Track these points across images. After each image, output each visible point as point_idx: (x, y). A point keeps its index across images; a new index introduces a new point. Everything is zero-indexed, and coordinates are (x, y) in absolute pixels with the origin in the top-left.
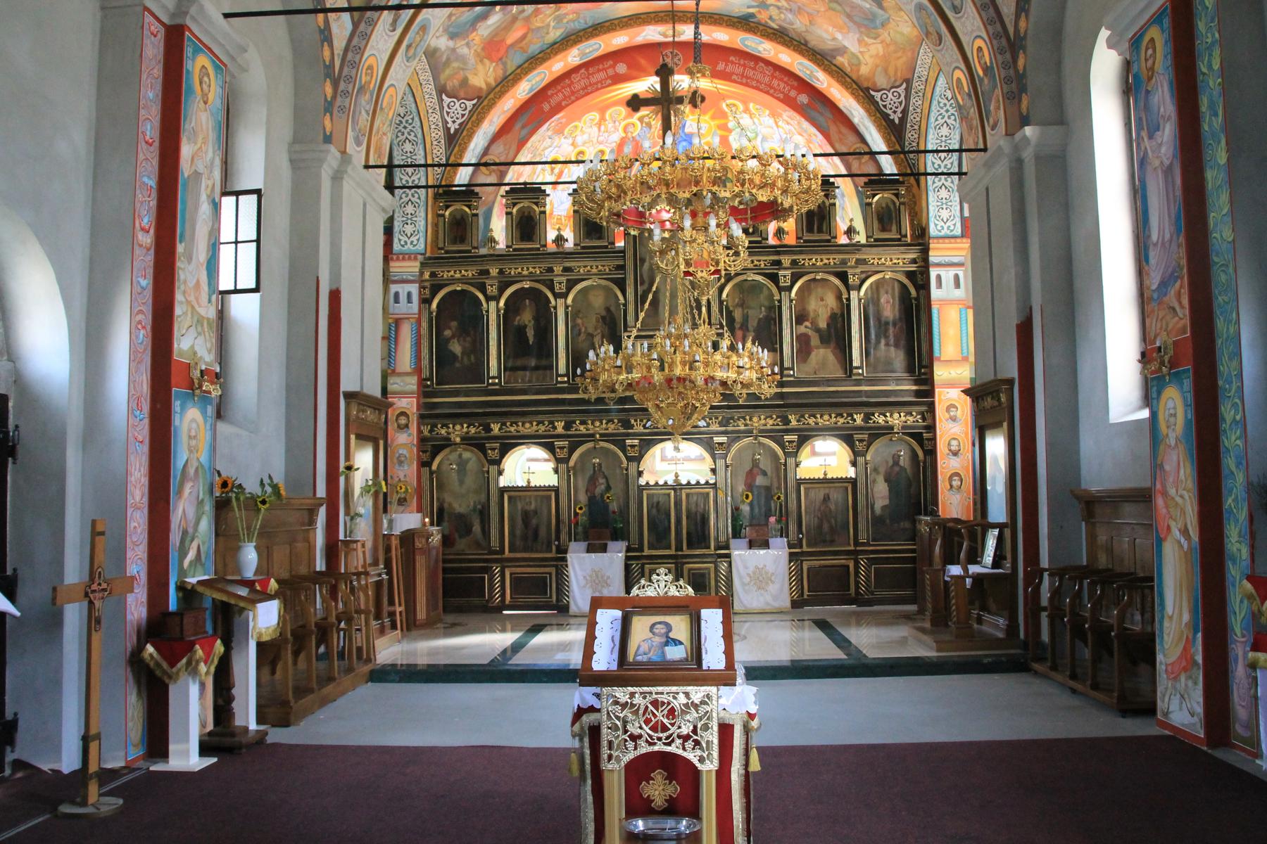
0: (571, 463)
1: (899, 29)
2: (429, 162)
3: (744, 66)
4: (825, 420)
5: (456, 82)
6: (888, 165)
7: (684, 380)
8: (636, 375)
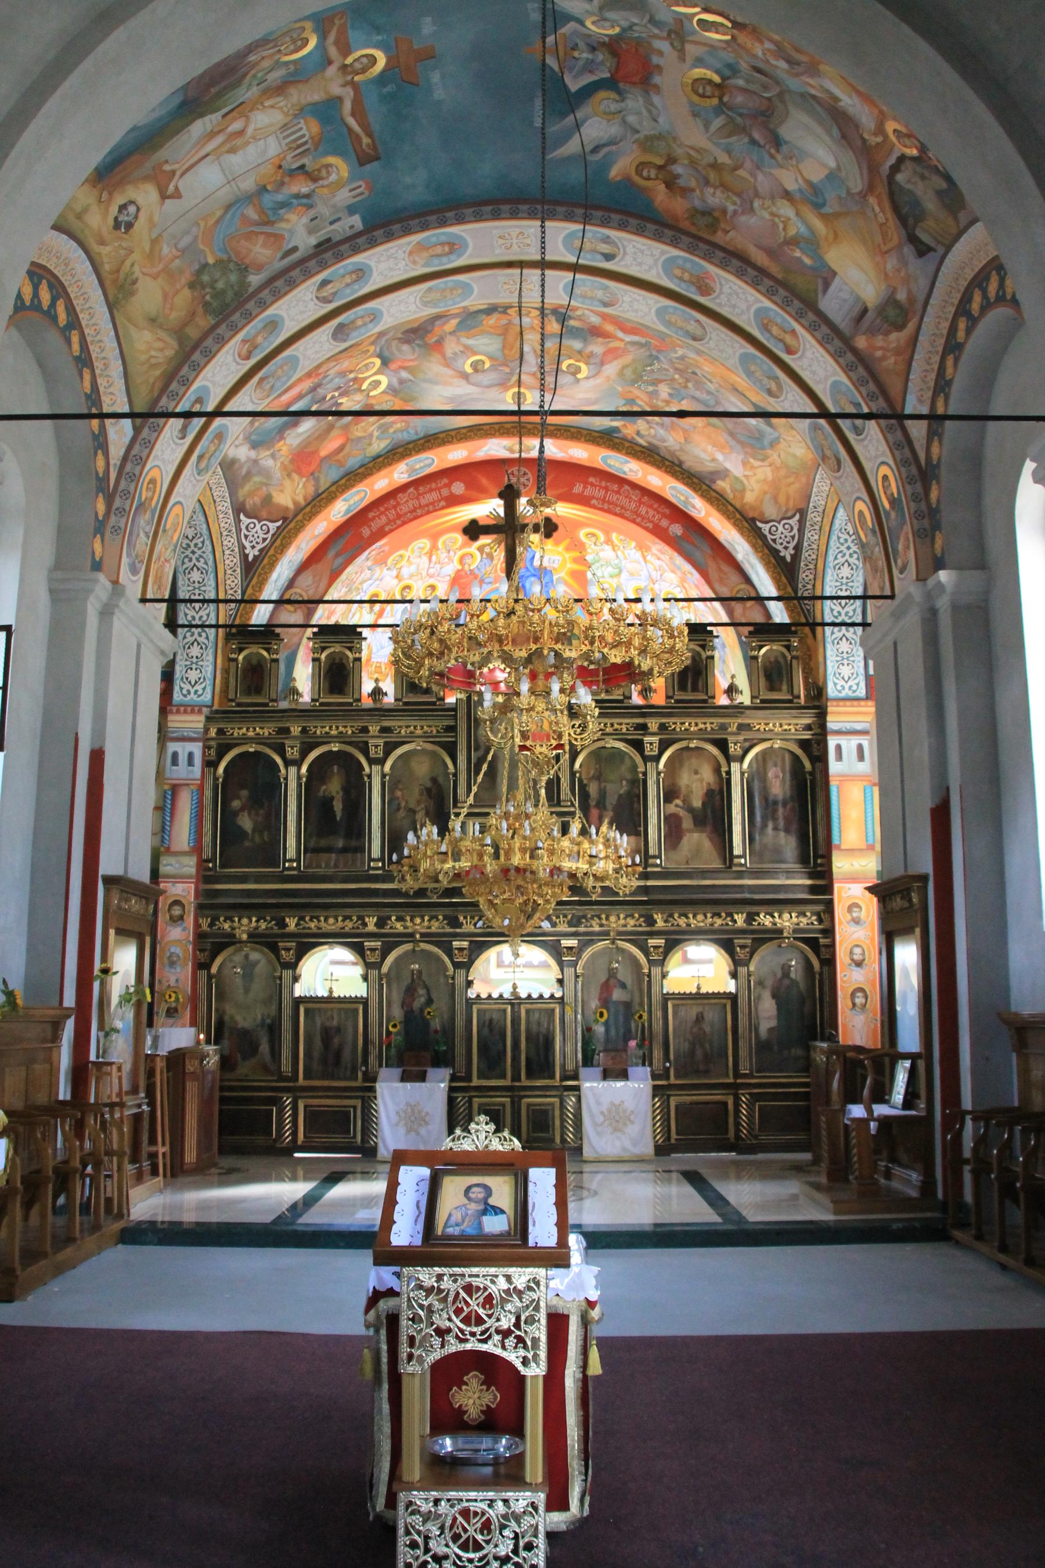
0: (385, 969)
2: (222, 596)
3: (606, 489)
4: (698, 921)
5: (257, 500)
6: (779, 613)
7: (525, 870)
8: (465, 864)
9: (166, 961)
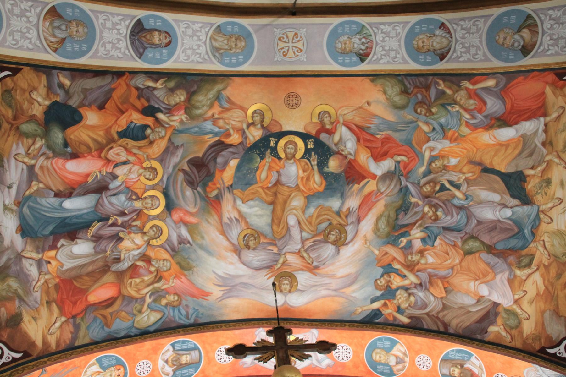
1: (553, 227)
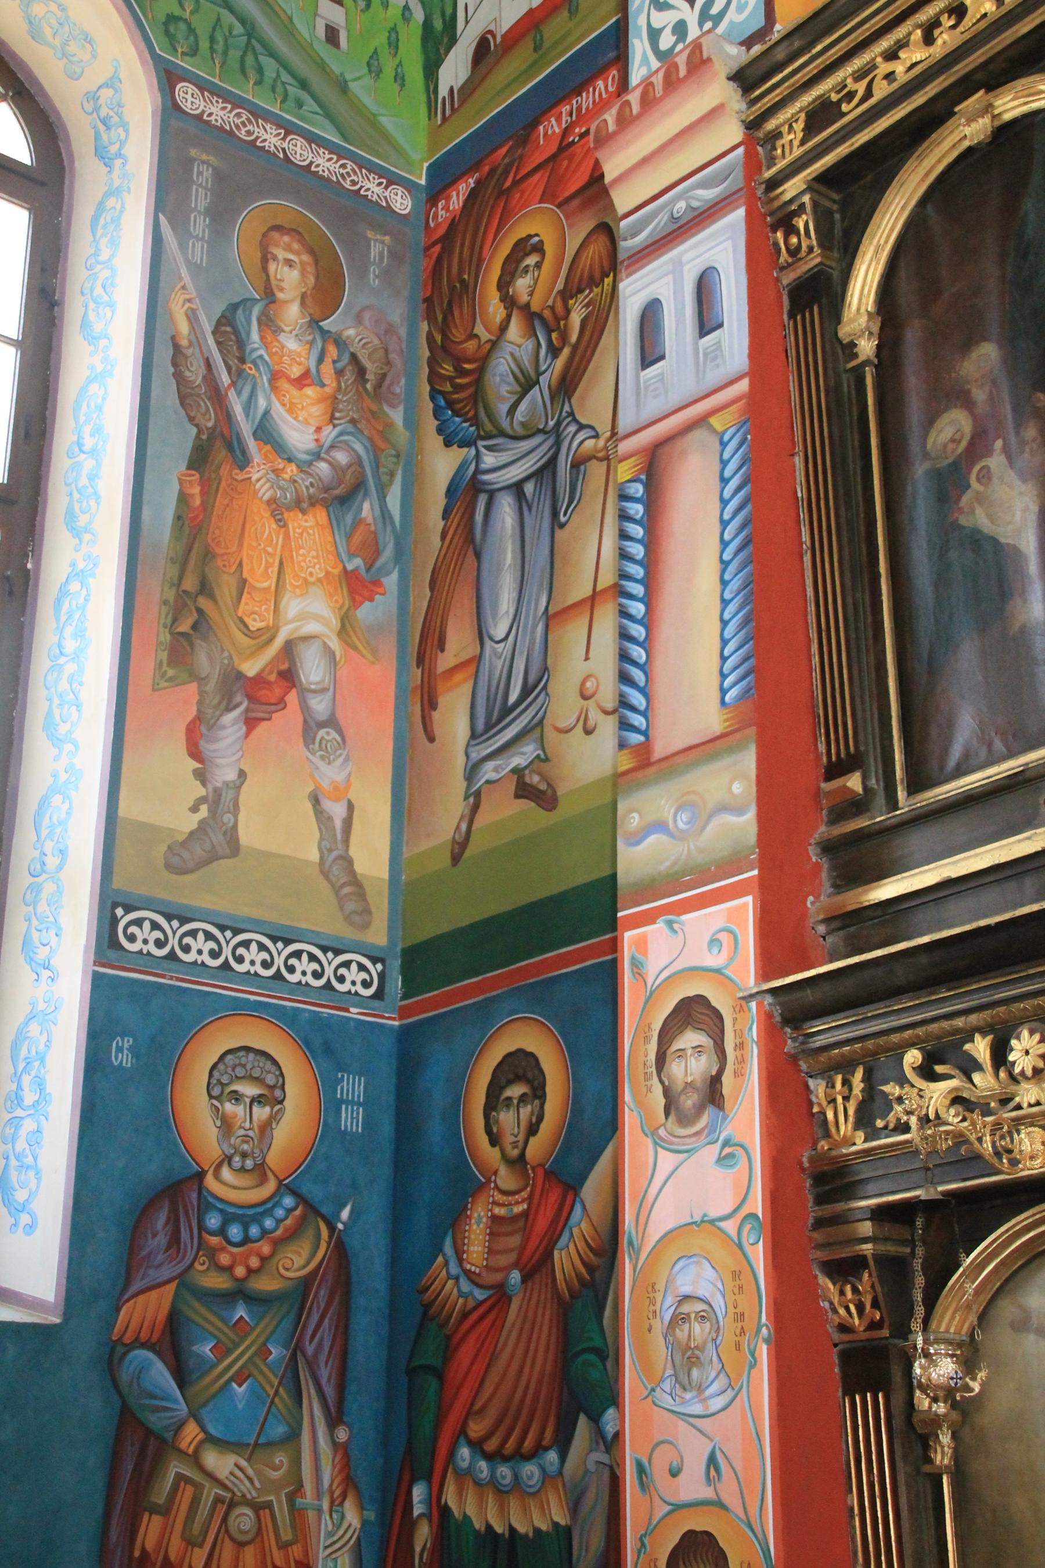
9: (660, 1351)
